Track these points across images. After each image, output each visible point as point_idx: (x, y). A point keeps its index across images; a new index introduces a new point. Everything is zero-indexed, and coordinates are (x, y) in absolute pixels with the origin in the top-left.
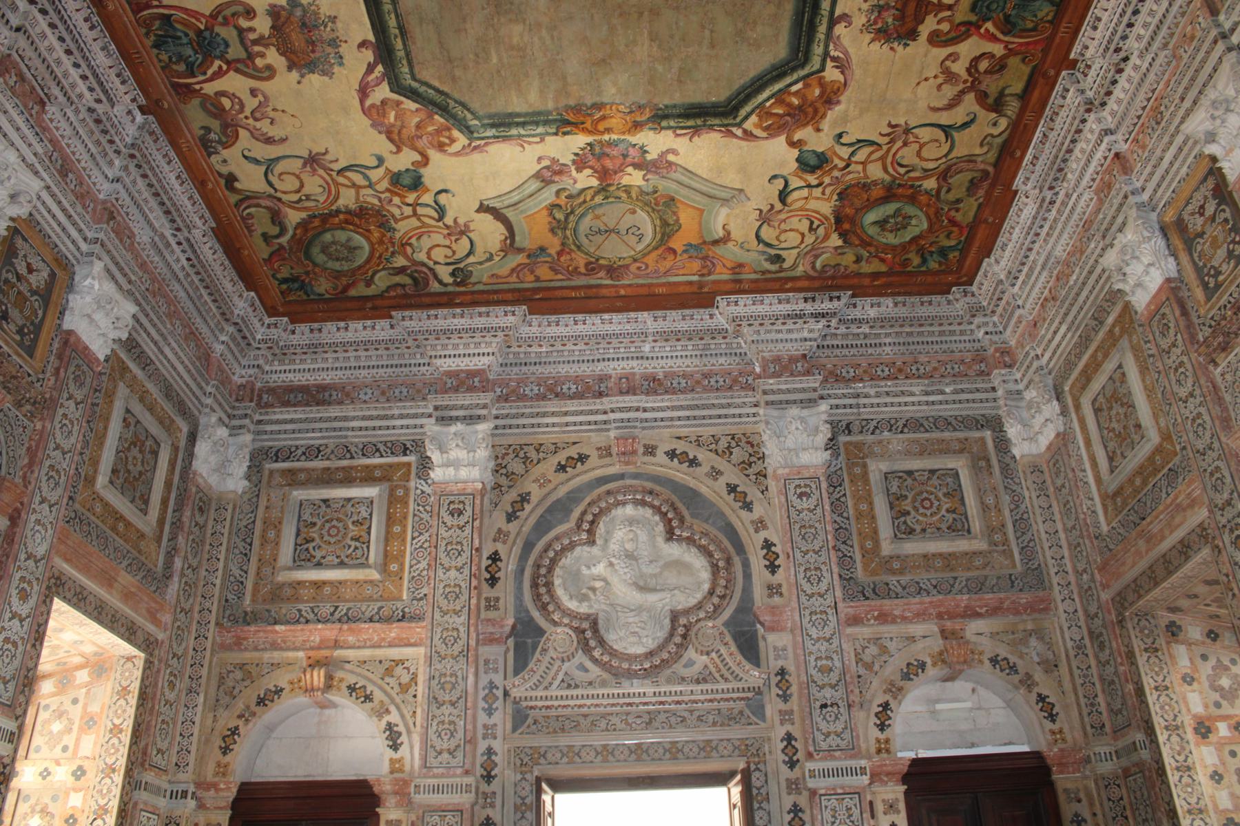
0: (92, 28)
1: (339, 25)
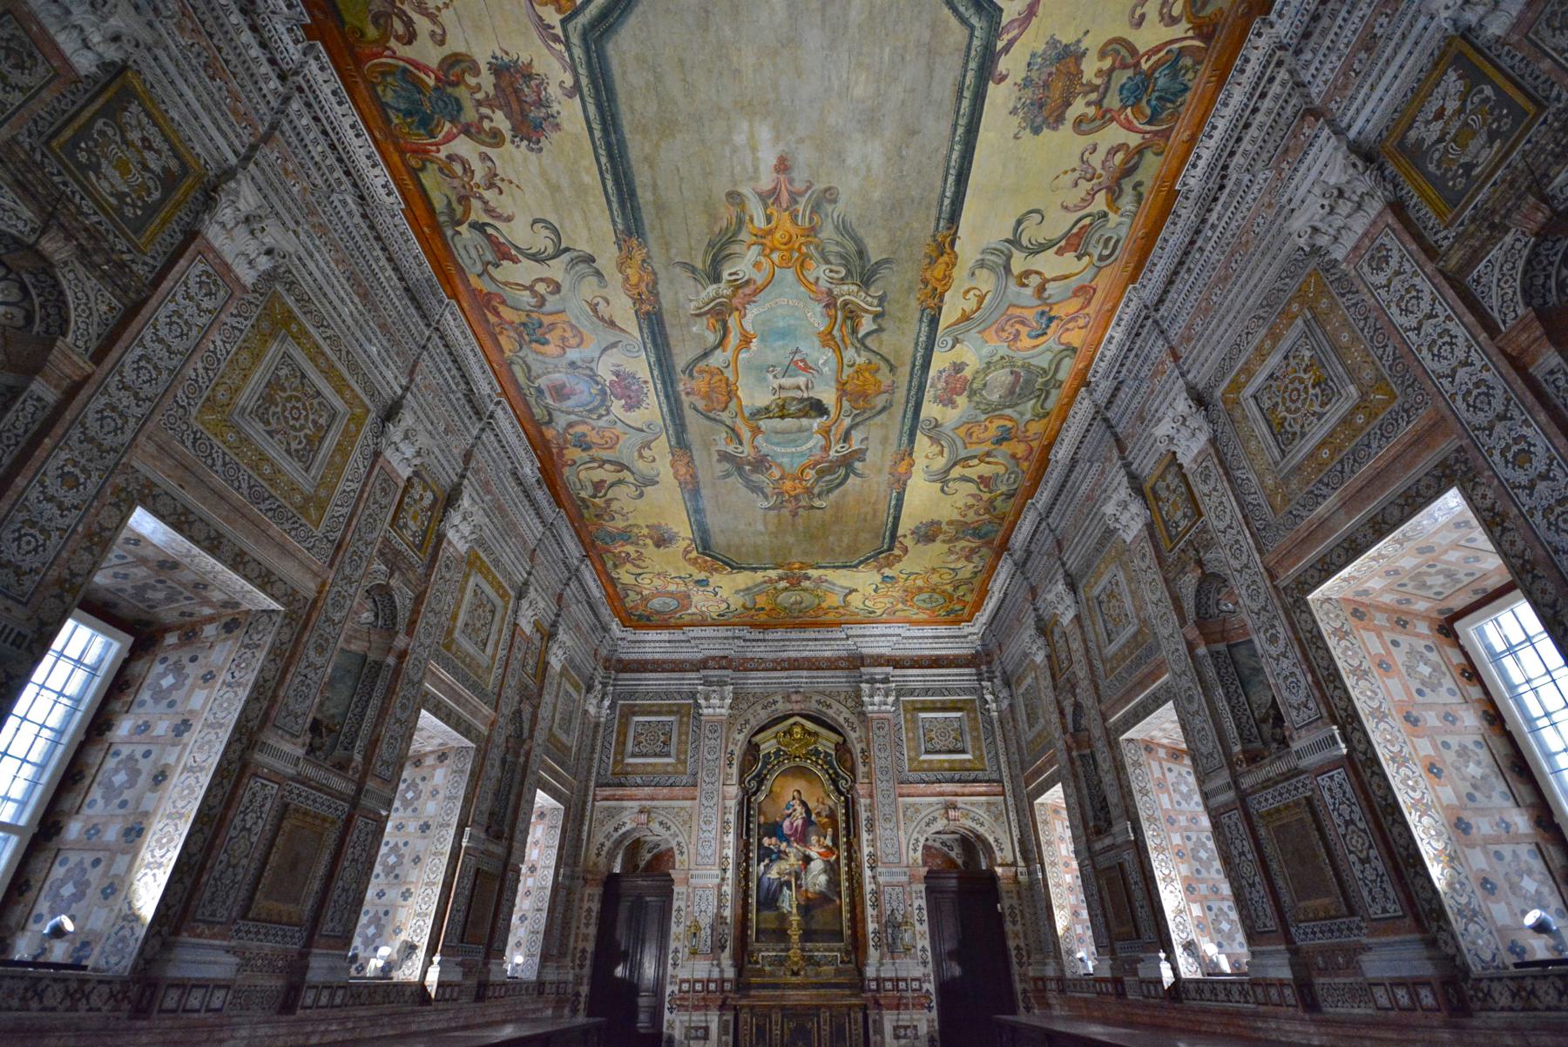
0: (1214, 128)
1: (1011, 106)
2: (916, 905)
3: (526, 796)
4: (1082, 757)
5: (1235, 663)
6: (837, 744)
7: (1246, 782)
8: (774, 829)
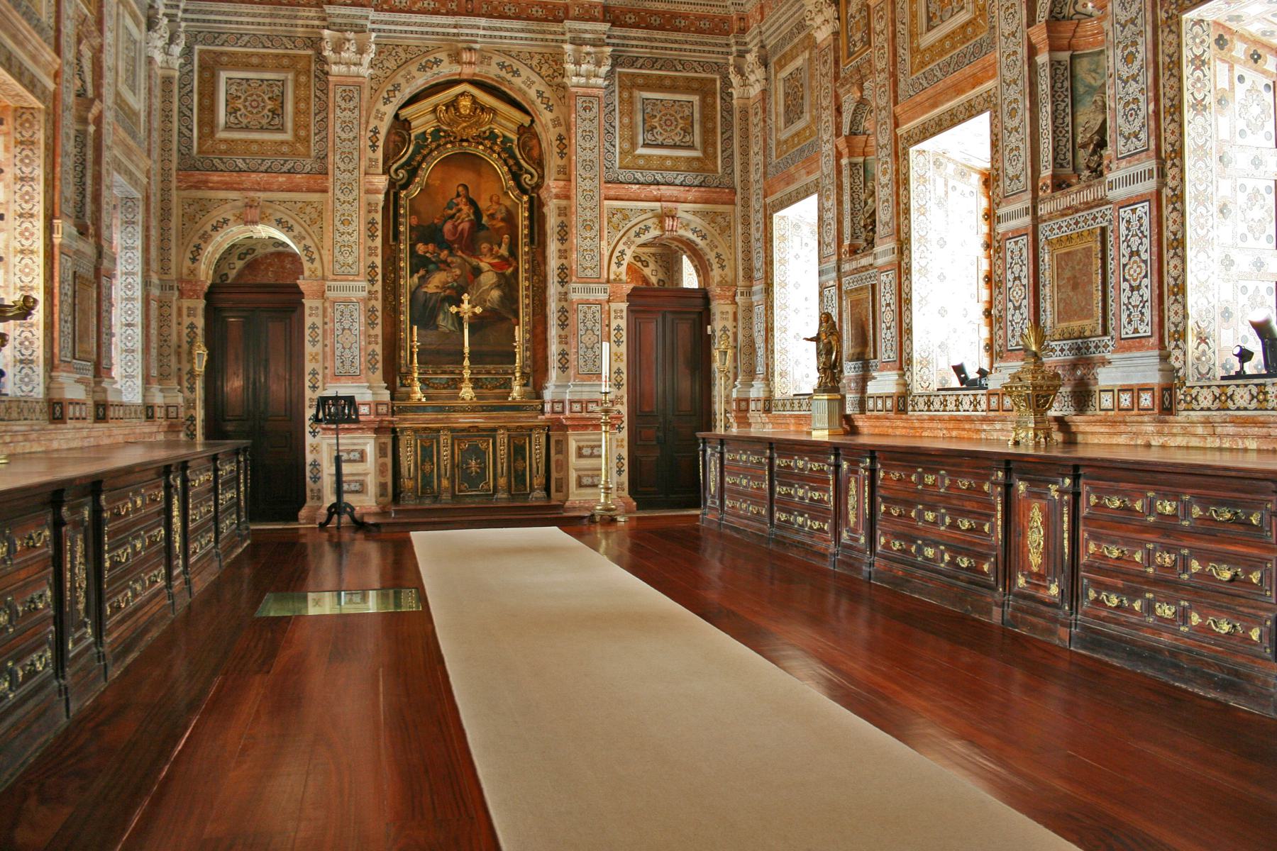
2: (613, 325)
3: (106, 180)
4: (853, 165)
5: (1073, 76)
6: (522, 129)
7: (1044, 209)
8: (428, 233)
